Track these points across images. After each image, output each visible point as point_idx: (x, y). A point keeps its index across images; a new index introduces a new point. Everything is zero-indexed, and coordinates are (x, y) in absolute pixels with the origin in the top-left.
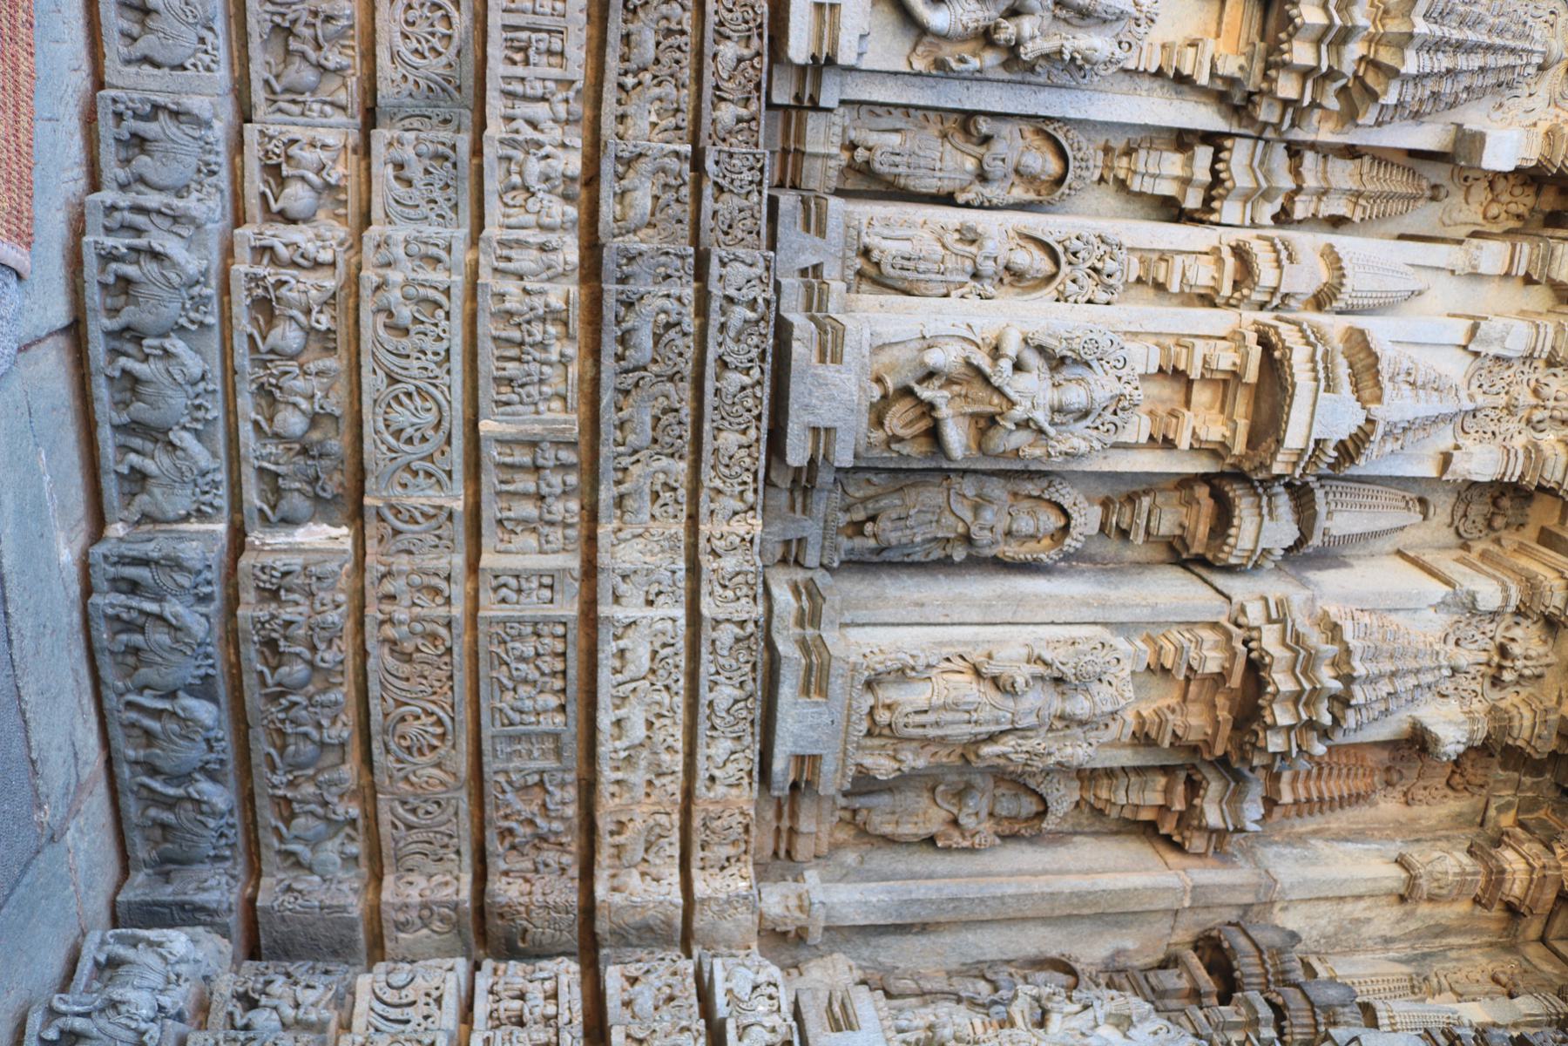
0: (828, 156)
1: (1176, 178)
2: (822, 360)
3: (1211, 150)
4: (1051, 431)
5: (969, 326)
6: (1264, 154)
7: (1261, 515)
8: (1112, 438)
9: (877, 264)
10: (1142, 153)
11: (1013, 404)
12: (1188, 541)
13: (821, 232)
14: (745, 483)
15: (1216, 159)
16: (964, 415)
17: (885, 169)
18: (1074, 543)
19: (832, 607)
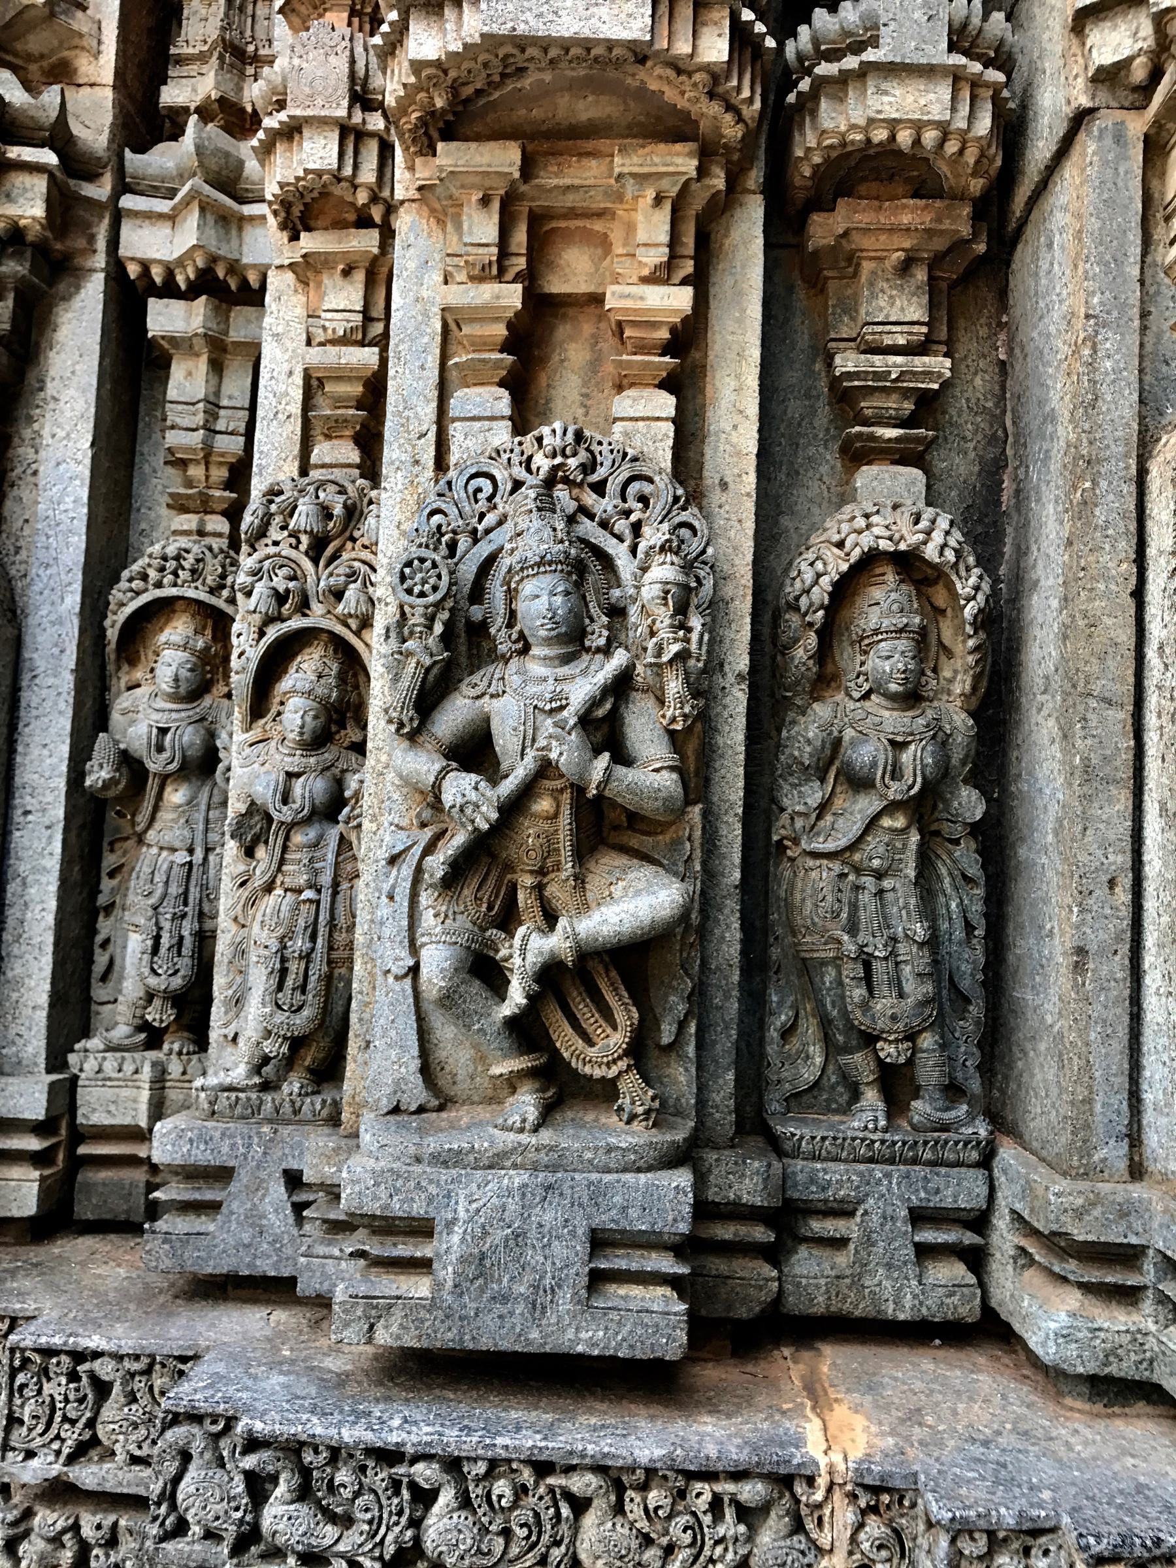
0: (160, 1080)
1: (217, 367)
2: (423, 1265)
3: (154, 304)
4: (619, 658)
5: (393, 860)
6: (153, 192)
7: (866, 70)
8: (663, 488)
9: (297, 1044)
10: (173, 438)
11: (545, 768)
12: (940, 244)
13: (222, 1175)
14: (716, 1505)
15: (169, 290)
16: (580, 880)
17: (185, 963)
18: (937, 537)
19: (1079, 1214)
